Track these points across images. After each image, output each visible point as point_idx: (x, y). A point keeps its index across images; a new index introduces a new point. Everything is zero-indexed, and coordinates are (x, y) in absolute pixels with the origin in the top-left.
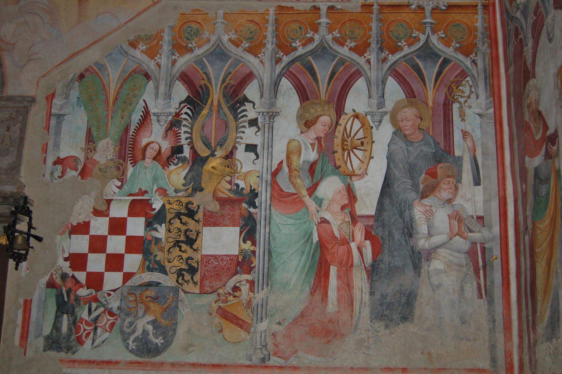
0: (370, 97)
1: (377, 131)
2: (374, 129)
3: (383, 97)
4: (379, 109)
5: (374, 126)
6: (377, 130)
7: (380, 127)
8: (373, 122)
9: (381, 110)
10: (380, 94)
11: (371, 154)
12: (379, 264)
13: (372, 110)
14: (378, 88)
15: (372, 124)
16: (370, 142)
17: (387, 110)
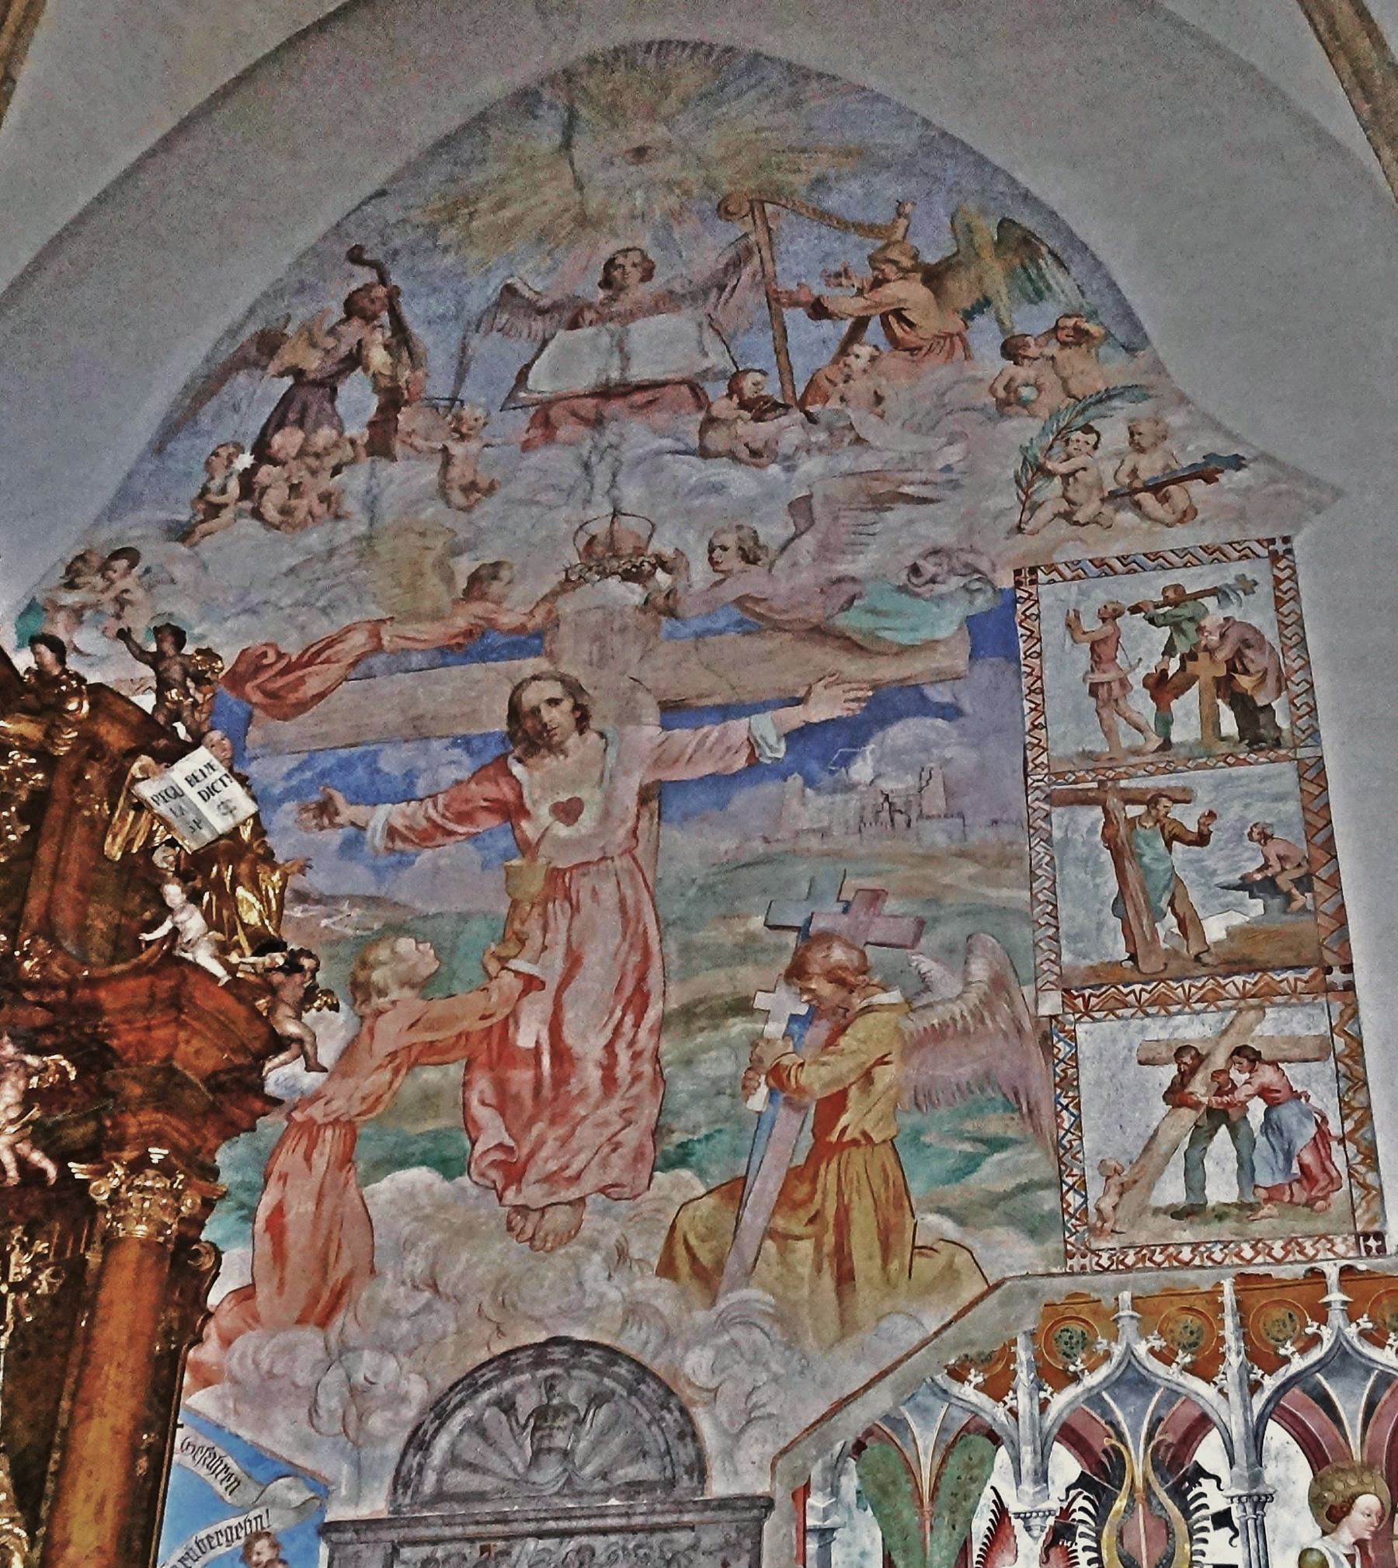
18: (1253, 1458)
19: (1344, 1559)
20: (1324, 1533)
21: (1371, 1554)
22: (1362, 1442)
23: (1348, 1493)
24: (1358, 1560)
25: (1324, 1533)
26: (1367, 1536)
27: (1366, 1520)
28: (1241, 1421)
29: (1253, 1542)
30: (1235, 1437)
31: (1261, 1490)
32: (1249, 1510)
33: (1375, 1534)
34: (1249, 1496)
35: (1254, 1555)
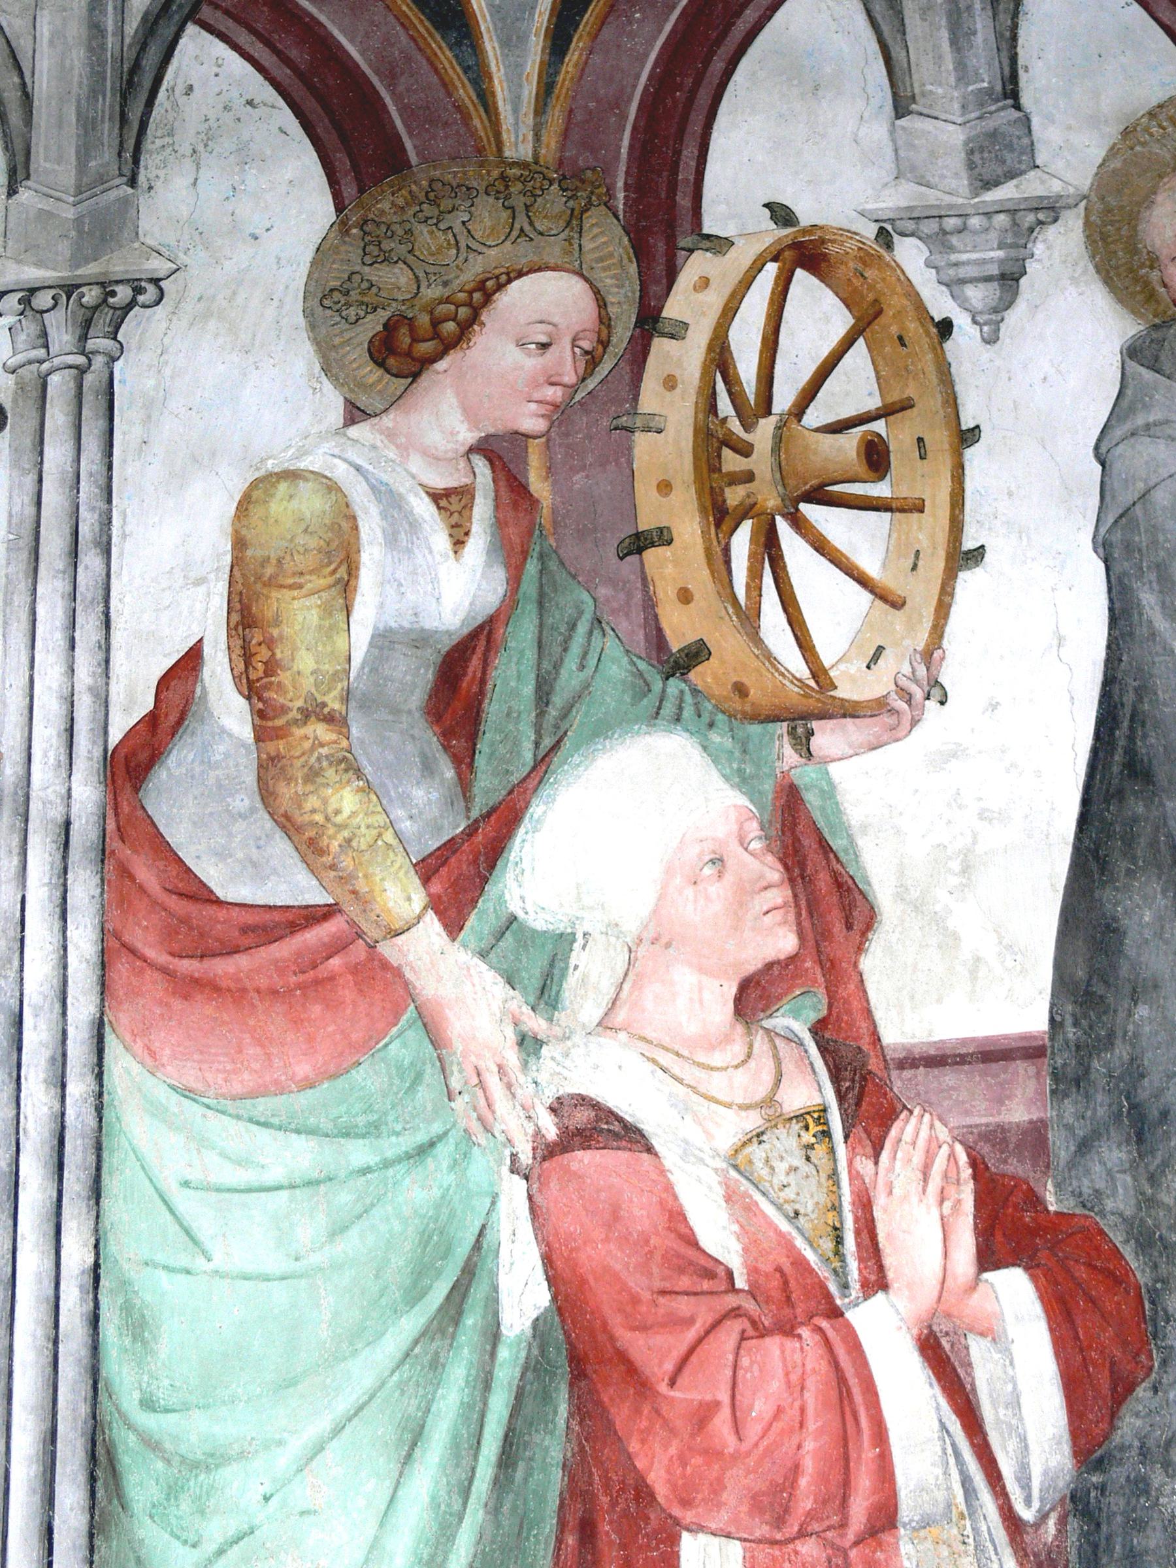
0: (902, 106)
1: (986, 354)
2: (965, 331)
3: (1011, 91)
4: (989, 184)
5: (961, 321)
6: (991, 340)
7: (1014, 317)
8: (954, 285)
9: (1006, 192)
10: (987, 77)
11: (956, 526)
12: (1140, 1486)
13: (932, 197)
14: (959, 36)
15: (940, 305)
16: (939, 439)
17: (1056, 187)
18: (105, 158)
19: (423, 508)
20: (355, 414)
21: (538, 485)
22: (547, 89)
23: (475, 268)
24: (482, 510)
25: (355, 414)
26: (531, 421)
27: (531, 363)
28: (76, 29)
29: (56, 454)
30: (43, 85)
31: (117, 264)
32: (62, 337)
33: (560, 414)
34: (70, 289)
35: (53, 497)
